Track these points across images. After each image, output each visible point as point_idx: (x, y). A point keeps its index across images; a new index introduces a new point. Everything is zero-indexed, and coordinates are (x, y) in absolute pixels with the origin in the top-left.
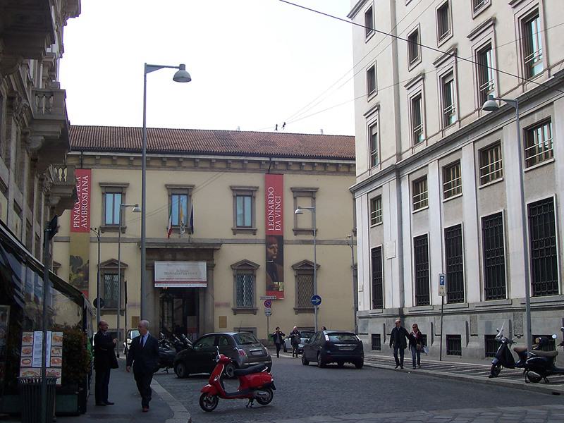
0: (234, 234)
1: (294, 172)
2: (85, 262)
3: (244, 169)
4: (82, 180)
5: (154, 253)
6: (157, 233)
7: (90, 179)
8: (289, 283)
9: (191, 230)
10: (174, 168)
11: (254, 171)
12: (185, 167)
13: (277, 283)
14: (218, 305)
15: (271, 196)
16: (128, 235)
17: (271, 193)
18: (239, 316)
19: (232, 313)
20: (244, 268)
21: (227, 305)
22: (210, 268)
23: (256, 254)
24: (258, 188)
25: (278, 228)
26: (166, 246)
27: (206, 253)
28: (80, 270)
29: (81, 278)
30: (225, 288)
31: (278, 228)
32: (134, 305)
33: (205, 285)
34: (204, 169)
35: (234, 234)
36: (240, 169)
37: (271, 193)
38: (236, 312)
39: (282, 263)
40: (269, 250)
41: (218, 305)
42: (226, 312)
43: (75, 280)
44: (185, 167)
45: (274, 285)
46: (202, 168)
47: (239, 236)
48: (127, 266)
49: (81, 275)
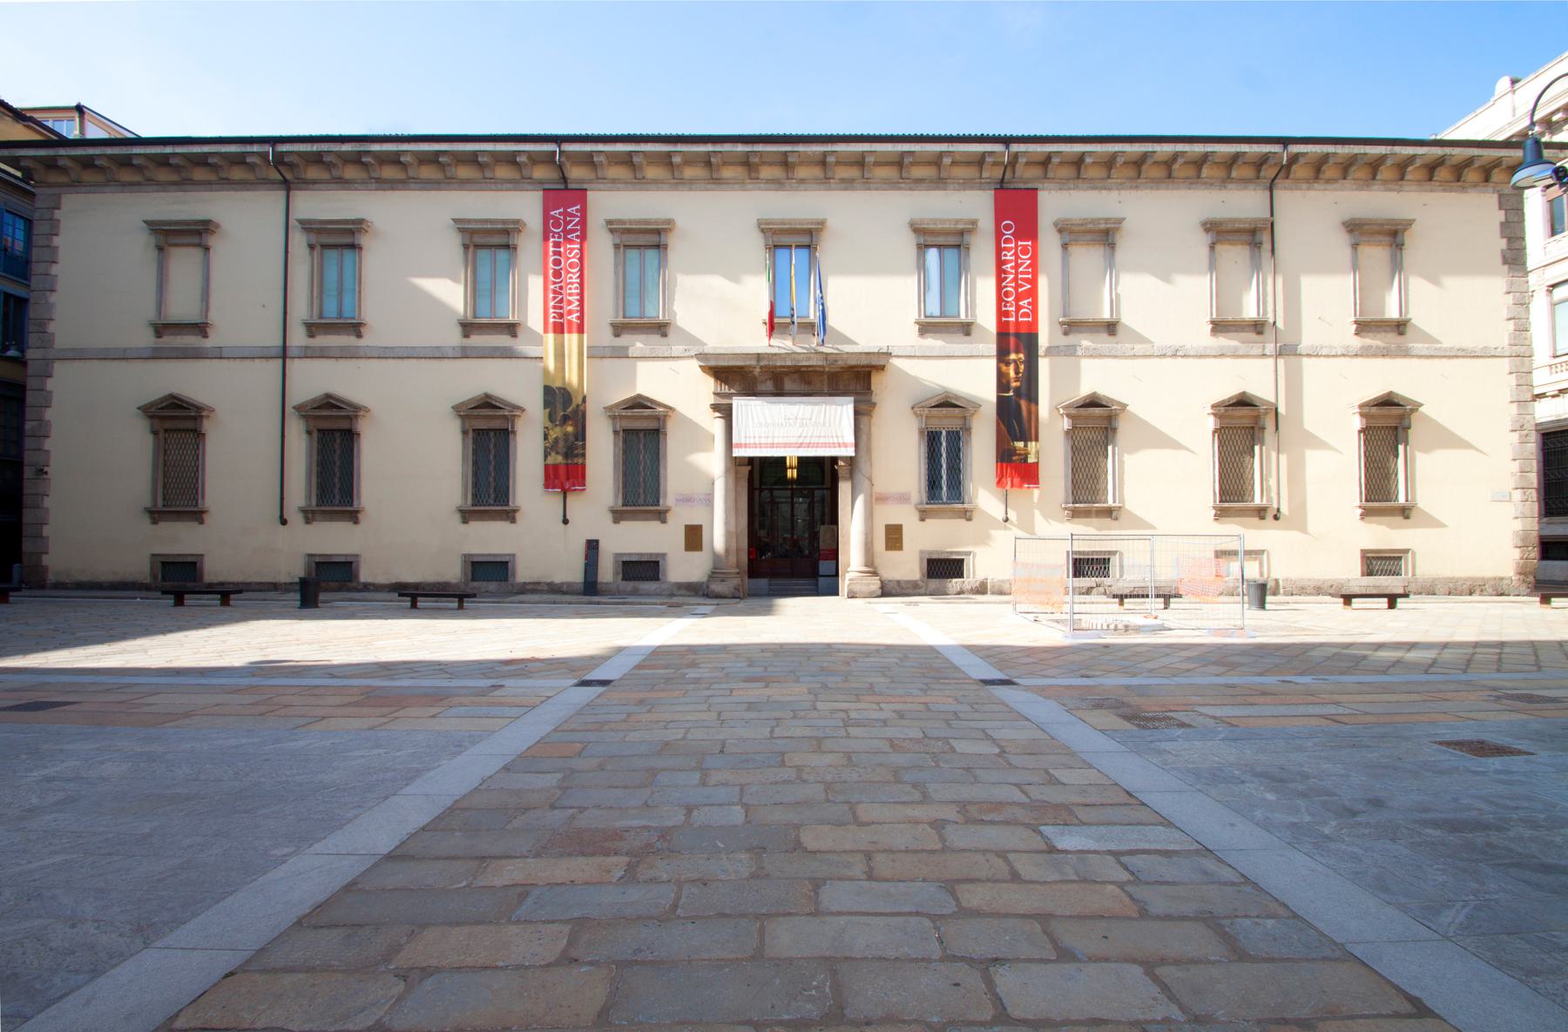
1: (1063, 184)
2: (577, 400)
3: (940, 183)
4: (565, 214)
5: (738, 378)
6: (746, 336)
7: (583, 211)
8: (1050, 448)
10: (777, 184)
11: (967, 184)
12: (802, 181)
13: (1020, 444)
15: (1007, 241)
17: (1008, 234)
19: (916, 516)
20: (944, 411)
21: (903, 498)
22: (862, 414)
23: (975, 377)
24: (974, 223)
25: (1026, 315)
27: (854, 379)
28: (565, 419)
29: (566, 434)
30: (899, 460)
31: (1026, 315)
33: (850, 452)
34: (848, 184)
37: (1008, 234)
38: (924, 515)
39: (1033, 398)
40: (1004, 368)
43: (556, 440)
44: (802, 181)
45: (1015, 449)
46: (843, 180)
49: (570, 429)
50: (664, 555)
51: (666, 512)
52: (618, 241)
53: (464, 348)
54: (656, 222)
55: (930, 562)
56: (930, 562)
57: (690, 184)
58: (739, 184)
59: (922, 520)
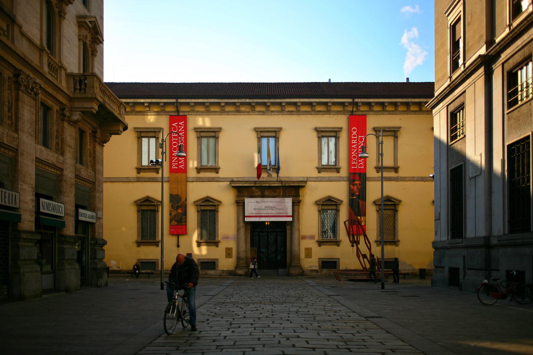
0: (319, 172)
3: (328, 112)
9: (277, 169)
10: (263, 113)
14: (304, 238)
16: (222, 174)
18: (324, 247)
19: (316, 245)
21: (312, 237)
26: (255, 183)
32: (226, 238)
34: (291, 113)
35: (319, 172)
36: (324, 111)
38: (320, 243)
41: (304, 238)
42: (312, 244)
44: (273, 111)
46: (288, 111)
47: (323, 174)
48: (221, 202)
50: (217, 259)
51: (219, 242)
52: (199, 136)
53: (138, 178)
54: (214, 128)
55: (323, 262)
56: (323, 262)
57: (228, 113)
58: (248, 113)
59: (320, 246)
